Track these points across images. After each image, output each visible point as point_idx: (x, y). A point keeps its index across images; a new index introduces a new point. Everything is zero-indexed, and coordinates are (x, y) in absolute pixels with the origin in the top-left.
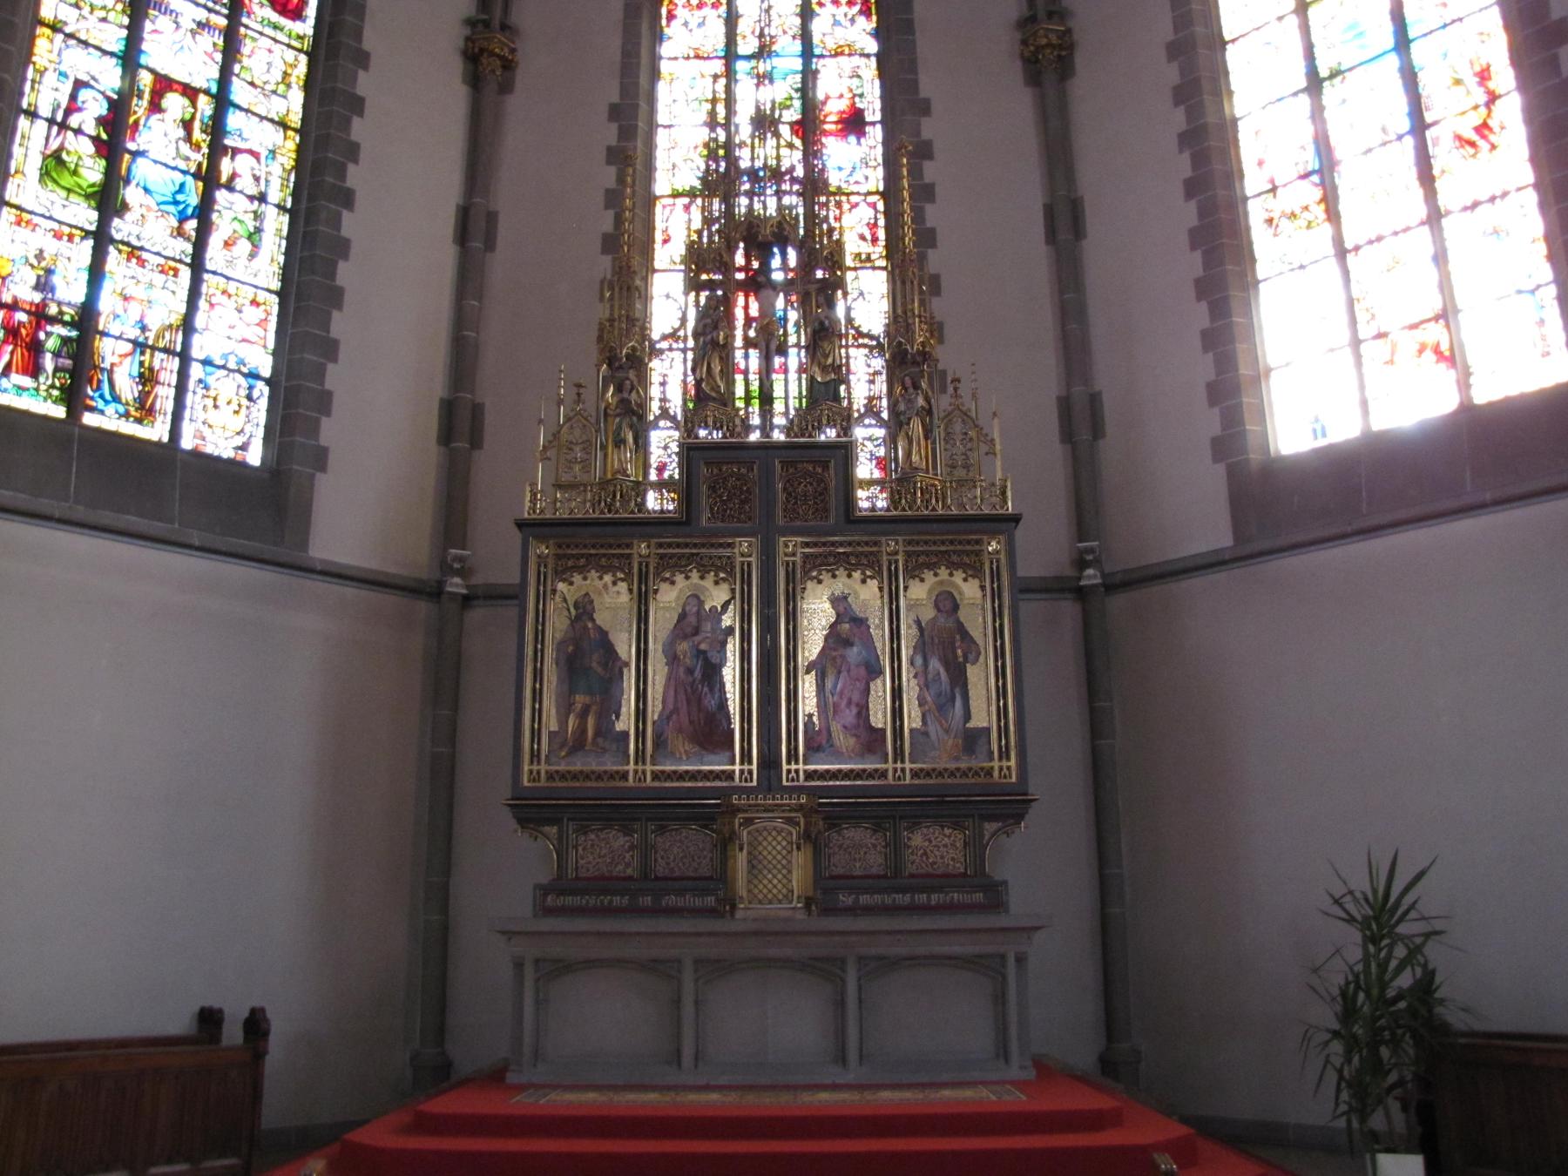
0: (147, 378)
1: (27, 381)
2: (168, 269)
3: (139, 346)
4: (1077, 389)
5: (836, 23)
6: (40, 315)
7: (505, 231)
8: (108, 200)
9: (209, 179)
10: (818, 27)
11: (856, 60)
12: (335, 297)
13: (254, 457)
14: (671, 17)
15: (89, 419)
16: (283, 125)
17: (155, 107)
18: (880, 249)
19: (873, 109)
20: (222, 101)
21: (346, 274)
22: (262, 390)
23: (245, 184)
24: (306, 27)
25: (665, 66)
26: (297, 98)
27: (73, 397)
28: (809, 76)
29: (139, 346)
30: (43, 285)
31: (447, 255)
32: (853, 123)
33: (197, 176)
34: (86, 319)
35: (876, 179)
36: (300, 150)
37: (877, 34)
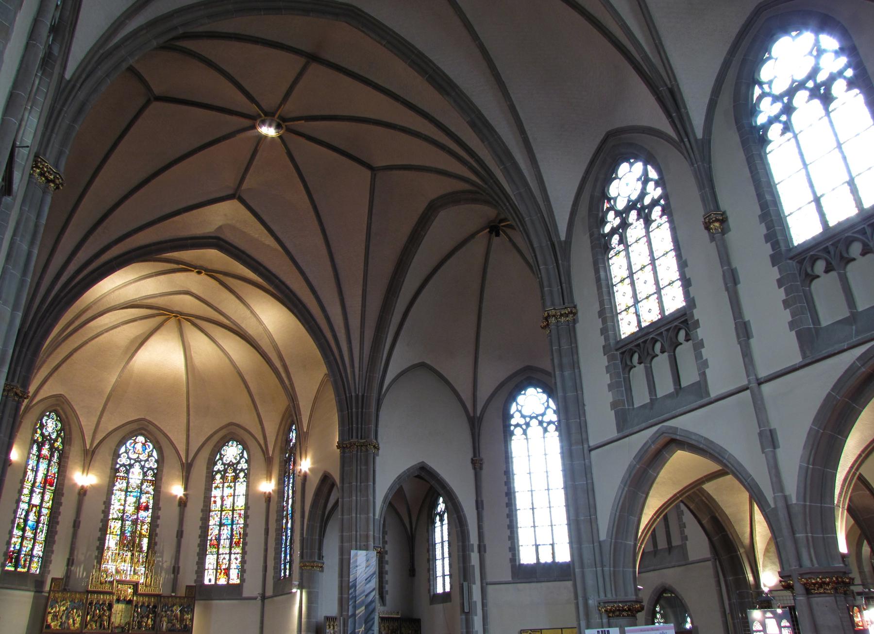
0: (25, 561)
1: (10, 564)
2: (30, 540)
3: (25, 555)
4: (176, 566)
5: (147, 487)
6: (13, 552)
7: (81, 525)
8: (24, 530)
9: (38, 522)
10: (144, 487)
11: (149, 495)
12: (54, 542)
13: (38, 572)
14: (117, 481)
15: (19, 570)
16: (48, 508)
17: (32, 510)
18: (148, 534)
19: (151, 506)
20: (41, 506)
21: (57, 537)
22: (40, 559)
23: (42, 522)
24: (53, 488)
25: (114, 491)
26: (51, 502)
27: (16, 566)
28: (140, 498)
29: (25, 555)
30: (14, 547)
31: (71, 530)
32: (146, 508)
33: (36, 522)
34: (20, 551)
35: (148, 520)
36: (50, 513)
37: (154, 490)
